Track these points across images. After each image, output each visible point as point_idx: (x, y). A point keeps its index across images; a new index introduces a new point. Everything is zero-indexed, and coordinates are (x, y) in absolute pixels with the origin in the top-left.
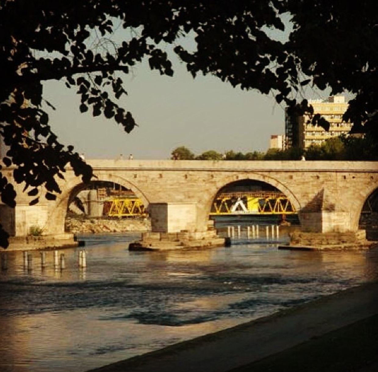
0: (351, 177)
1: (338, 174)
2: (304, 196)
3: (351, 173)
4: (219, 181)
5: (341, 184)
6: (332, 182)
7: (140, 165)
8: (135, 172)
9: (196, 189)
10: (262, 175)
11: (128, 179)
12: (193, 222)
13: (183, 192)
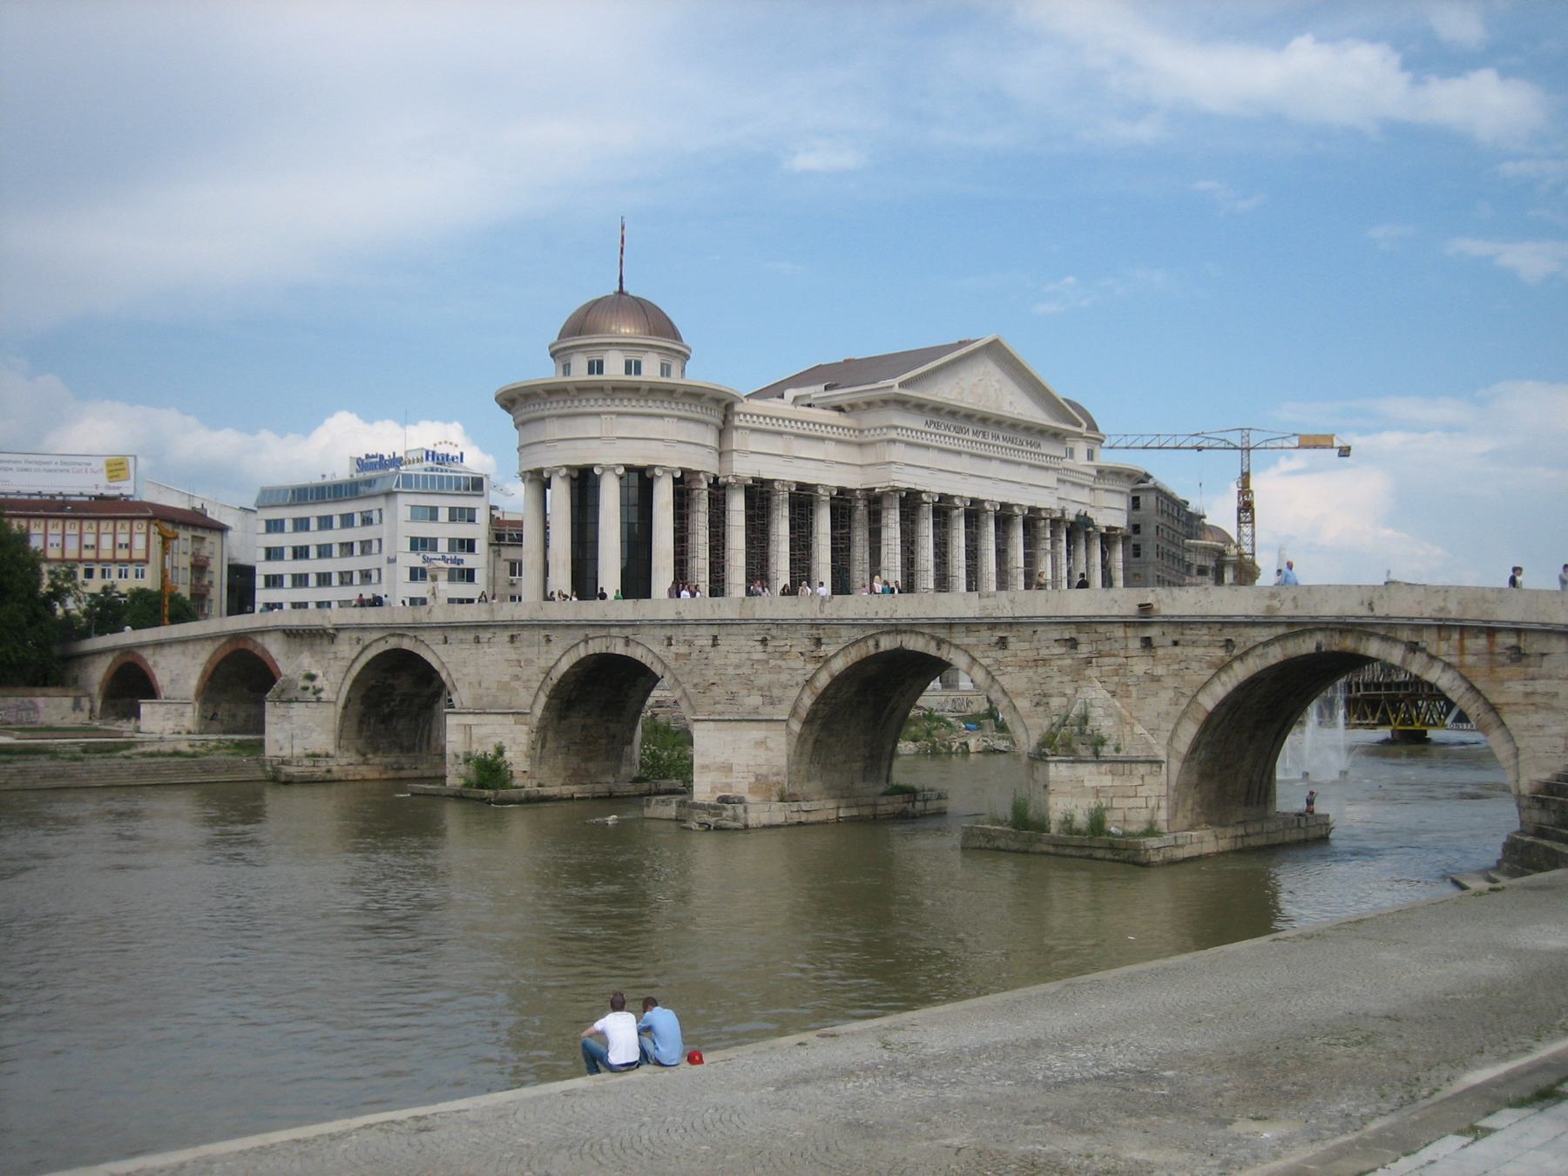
0: (1168, 641)
1: (1130, 632)
2: (1038, 704)
4: (835, 655)
5: (1140, 666)
6: (1113, 660)
7: (678, 613)
8: (668, 632)
9: (784, 677)
10: (933, 637)
11: (656, 650)
12: (778, 774)
13: (761, 689)
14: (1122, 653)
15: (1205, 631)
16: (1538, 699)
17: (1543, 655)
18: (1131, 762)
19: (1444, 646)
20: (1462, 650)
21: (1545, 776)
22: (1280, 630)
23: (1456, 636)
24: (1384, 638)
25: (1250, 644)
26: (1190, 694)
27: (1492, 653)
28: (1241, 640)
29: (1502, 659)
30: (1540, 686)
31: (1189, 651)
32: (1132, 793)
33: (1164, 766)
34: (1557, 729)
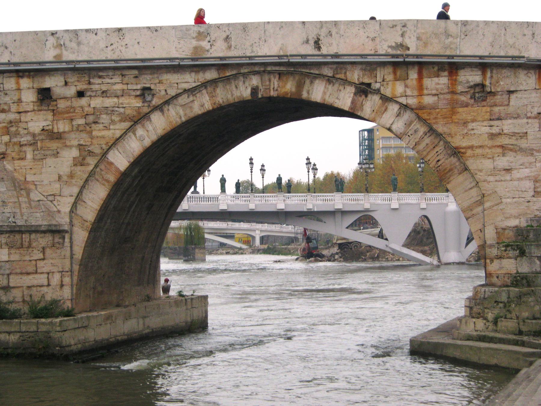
0: (72, 91)
1: (25, 83)
3: (72, 78)
5: (37, 122)
14: (14, 108)
15: (117, 79)
16: (505, 141)
17: (510, 92)
18: (30, 232)
19: (399, 88)
20: (420, 87)
21: (514, 223)
22: (211, 75)
23: (413, 75)
24: (330, 80)
25: (172, 92)
26: (98, 151)
27: (453, 93)
28: (162, 87)
29: (463, 98)
30: (508, 126)
31: (97, 102)
32: (31, 269)
33: (67, 236)
34: (526, 172)
